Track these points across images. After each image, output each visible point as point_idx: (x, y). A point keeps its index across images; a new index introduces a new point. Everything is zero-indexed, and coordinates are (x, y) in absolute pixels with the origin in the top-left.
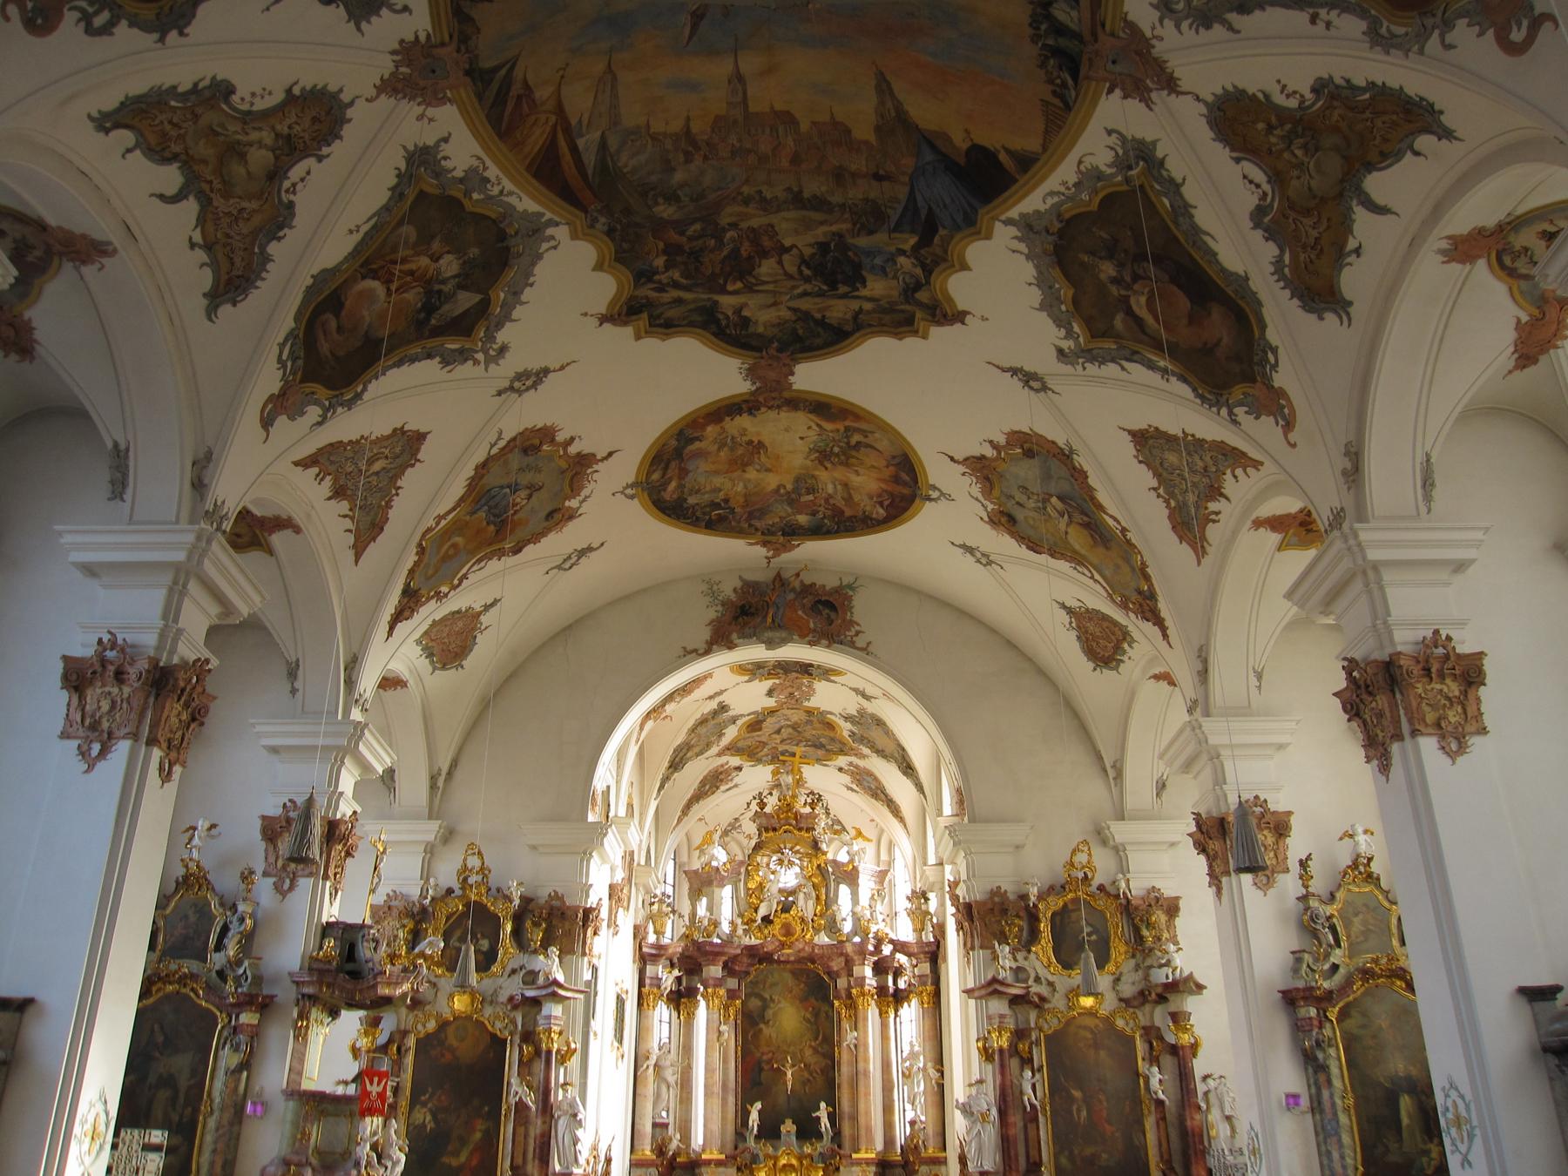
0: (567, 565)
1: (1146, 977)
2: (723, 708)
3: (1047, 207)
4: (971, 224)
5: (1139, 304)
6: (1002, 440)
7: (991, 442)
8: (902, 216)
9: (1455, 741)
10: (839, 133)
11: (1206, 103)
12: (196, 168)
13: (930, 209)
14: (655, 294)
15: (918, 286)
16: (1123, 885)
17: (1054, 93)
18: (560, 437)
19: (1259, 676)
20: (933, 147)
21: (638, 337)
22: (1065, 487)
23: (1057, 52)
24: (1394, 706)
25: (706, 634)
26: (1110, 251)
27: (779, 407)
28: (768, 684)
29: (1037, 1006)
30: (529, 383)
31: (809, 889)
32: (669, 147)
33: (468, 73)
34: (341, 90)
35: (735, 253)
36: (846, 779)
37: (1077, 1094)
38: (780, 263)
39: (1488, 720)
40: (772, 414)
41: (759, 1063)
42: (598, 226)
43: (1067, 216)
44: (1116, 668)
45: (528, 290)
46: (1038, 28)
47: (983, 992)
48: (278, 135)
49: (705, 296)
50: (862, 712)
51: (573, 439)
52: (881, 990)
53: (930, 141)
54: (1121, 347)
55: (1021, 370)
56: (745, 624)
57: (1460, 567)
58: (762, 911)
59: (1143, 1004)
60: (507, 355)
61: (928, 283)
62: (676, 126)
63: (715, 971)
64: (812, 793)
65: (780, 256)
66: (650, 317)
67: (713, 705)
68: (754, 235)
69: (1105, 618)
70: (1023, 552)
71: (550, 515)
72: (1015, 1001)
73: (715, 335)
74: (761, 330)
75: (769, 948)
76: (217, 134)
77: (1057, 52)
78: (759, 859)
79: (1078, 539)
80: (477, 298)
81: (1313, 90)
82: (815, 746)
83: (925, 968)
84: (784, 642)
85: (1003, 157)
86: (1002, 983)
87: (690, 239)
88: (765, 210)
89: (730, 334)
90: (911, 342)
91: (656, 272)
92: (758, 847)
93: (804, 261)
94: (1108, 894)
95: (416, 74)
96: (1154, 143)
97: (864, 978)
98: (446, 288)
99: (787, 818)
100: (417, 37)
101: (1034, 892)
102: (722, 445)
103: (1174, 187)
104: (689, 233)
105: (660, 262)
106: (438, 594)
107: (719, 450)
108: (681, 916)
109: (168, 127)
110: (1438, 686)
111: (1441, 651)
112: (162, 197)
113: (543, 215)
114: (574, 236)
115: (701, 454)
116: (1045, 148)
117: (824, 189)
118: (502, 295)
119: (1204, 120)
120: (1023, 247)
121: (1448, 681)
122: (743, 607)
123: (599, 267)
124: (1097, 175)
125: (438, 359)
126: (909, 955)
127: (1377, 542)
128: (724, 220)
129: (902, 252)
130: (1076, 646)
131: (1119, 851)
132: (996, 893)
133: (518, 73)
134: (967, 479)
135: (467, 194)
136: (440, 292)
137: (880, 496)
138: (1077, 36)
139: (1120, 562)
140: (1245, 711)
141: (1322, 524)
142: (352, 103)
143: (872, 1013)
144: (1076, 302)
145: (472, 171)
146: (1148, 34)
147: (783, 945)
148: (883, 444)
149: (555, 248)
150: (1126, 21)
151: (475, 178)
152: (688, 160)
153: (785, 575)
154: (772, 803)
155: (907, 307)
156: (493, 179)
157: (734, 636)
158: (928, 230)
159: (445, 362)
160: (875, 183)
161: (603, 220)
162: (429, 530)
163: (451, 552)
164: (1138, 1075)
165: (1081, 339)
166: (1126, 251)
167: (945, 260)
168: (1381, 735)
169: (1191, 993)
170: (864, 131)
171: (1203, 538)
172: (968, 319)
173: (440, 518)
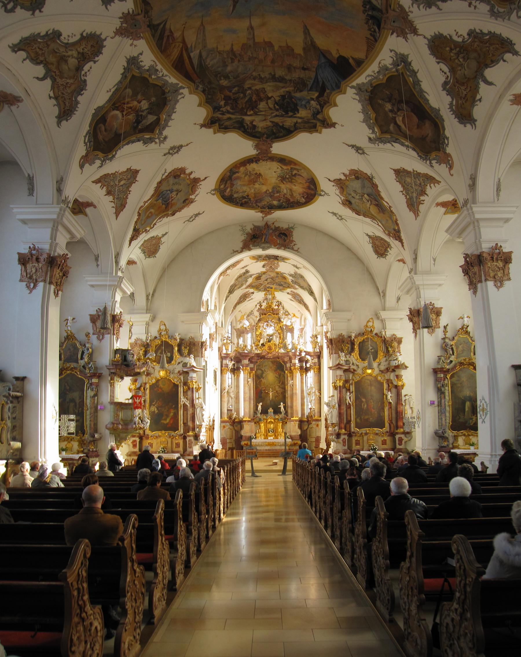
0: (191, 220)
1: (389, 364)
2: (247, 272)
3: (367, 81)
4: (338, 88)
5: (399, 120)
6: (347, 173)
7: (344, 174)
8: (313, 84)
9: (499, 283)
10: (289, 51)
11: (428, 39)
12: (49, 66)
13: (323, 81)
14: (220, 116)
15: (318, 113)
16: (384, 333)
17: (371, 34)
18: (187, 172)
19: (435, 260)
20: (325, 56)
21: (215, 133)
22: (369, 190)
23: (372, 17)
24: (480, 271)
25: (241, 245)
26: (390, 99)
27: (267, 160)
28: (263, 263)
29: (352, 373)
30: (175, 151)
31: (277, 334)
32: (225, 57)
33: (149, 26)
34: (101, 34)
35: (250, 99)
36: (290, 297)
37: (364, 400)
38: (267, 103)
39: (511, 275)
40: (264, 163)
41: (261, 391)
42: (199, 89)
43: (374, 85)
44: (385, 258)
45: (174, 114)
46: (365, 7)
47: (335, 368)
48: (79, 53)
49: (239, 117)
50: (296, 273)
51: (192, 172)
52: (301, 368)
53: (323, 54)
54: (392, 137)
55: (355, 146)
56: (255, 242)
57: (507, 220)
58: (261, 342)
59: (387, 372)
60: (167, 140)
61: (322, 111)
62: (228, 48)
63: (246, 362)
64: (278, 301)
65: (267, 101)
66: (219, 125)
67: (244, 270)
69: (382, 239)
70: (354, 215)
71: (184, 201)
72: (345, 371)
73: (243, 132)
74: (260, 130)
75: (264, 354)
76: (56, 52)
77: (372, 17)
78: (260, 324)
79: (373, 210)
80: (155, 117)
81: (468, 34)
82: (279, 285)
83: (316, 360)
84: (268, 248)
85: (351, 61)
86: (341, 365)
87: (234, 94)
88: (261, 82)
89: (249, 132)
90: (315, 135)
92: (260, 320)
93: (276, 103)
94: (378, 336)
95: (129, 27)
96: (408, 55)
97: (295, 364)
98: (144, 114)
99: (270, 310)
100: (129, 11)
101: (353, 335)
102: (246, 175)
103: (414, 73)
104: (233, 91)
105: (222, 103)
106: (146, 230)
107: (245, 176)
108: (234, 344)
109: (38, 50)
110: (496, 264)
111: (498, 251)
112: (37, 78)
113: (179, 84)
114: (190, 93)
115: (239, 178)
116: (367, 57)
117: (283, 73)
118: (164, 116)
119: (427, 46)
120: (357, 97)
121: (499, 262)
122: (254, 235)
123: (200, 105)
124: (386, 68)
125: (142, 142)
126: (311, 356)
127: (479, 211)
128: (246, 86)
129: (313, 99)
130: (371, 249)
131: (383, 321)
132: (341, 335)
133: (168, 26)
134: (335, 188)
135: (150, 76)
136: (141, 115)
137: (303, 194)
138: (380, 11)
139: (388, 219)
140: (428, 272)
141: (460, 205)
142: (105, 39)
143: (298, 375)
144: (376, 119)
145: (151, 67)
146: (407, 10)
147: (268, 353)
148: (305, 174)
149: (183, 97)
150: (399, 4)
151: (153, 70)
152: (232, 62)
153: (269, 223)
154: (264, 305)
156: (159, 70)
157: (251, 246)
158: (322, 91)
159: (145, 143)
160: (303, 71)
161: (201, 86)
162: (142, 207)
163: (150, 215)
164: (384, 394)
165: (378, 134)
166: (395, 99)
167: (328, 102)
168: (475, 281)
169: (404, 369)
170: (299, 50)
171: (418, 210)
172: (336, 126)
173: (145, 202)
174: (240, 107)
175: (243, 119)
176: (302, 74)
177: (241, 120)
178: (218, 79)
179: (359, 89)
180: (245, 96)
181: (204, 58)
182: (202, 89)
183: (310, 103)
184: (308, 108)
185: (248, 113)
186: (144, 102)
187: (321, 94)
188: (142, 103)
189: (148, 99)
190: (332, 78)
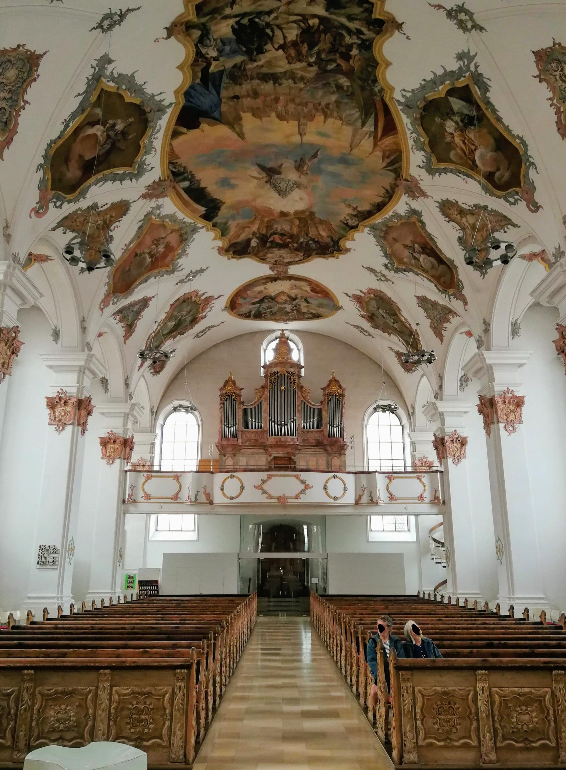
3: (158, 124)
11: (131, 203)
13: (208, 90)
14: (364, 30)
15: (201, 40)
23: (183, 173)
26: (124, 133)
33: (399, 176)
35: (311, 48)
38: (285, 38)
42: (379, 88)
45: (428, 79)
48: (462, 217)
49: (333, 17)
61: (196, 45)
62: (330, 120)
68: (299, 57)
80: (451, 99)
81: (112, 236)
85: (185, 130)
87: (335, 61)
88: (293, 73)
91: (359, 45)
93: (271, 39)
95: (415, 190)
96: (137, 180)
98: (457, 118)
103: (122, 178)
104: (334, 65)
105: (355, 52)
114: (392, 89)
116: (171, 144)
117: (262, 87)
119: (128, 199)
120: (158, 98)
128: (315, 69)
129: (216, 59)
133: (384, 164)
136: (462, 121)
142: (437, 202)
144: (121, 96)
149: (404, 90)
155: (203, 20)
156: (412, 140)
159: (487, 90)
160: (237, 94)
161: (376, 89)
166: (119, 141)
167: (192, 65)
174: (329, 35)
175: (327, 10)
176: (237, 90)
177: (332, 10)
178: (350, 88)
179: (161, 110)
180: (318, 54)
181: (360, 120)
182: (376, 84)
183: (218, 50)
184: (219, 41)
185: (316, 21)
186: (448, 130)
187: (205, 71)
188: (451, 131)
189: (442, 127)
190: (198, 99)
